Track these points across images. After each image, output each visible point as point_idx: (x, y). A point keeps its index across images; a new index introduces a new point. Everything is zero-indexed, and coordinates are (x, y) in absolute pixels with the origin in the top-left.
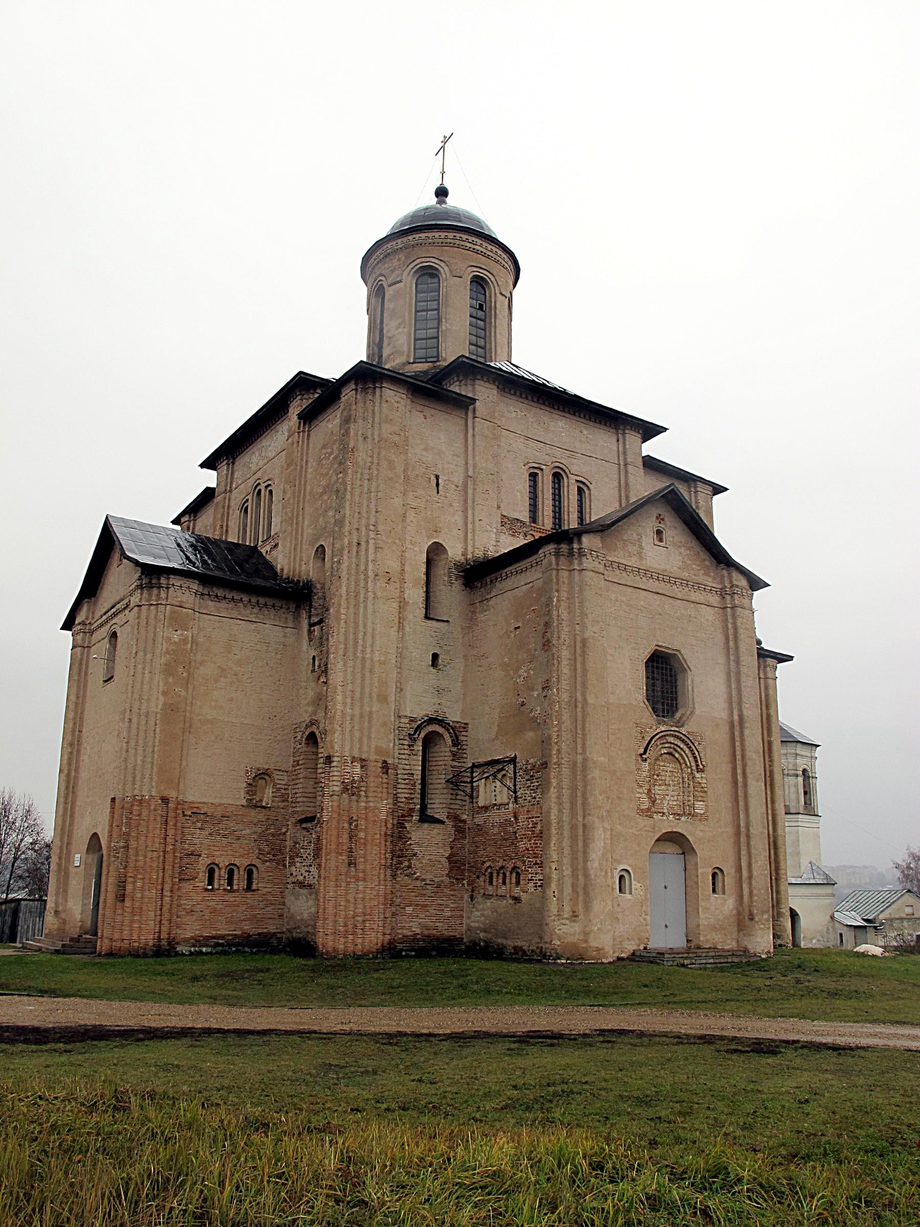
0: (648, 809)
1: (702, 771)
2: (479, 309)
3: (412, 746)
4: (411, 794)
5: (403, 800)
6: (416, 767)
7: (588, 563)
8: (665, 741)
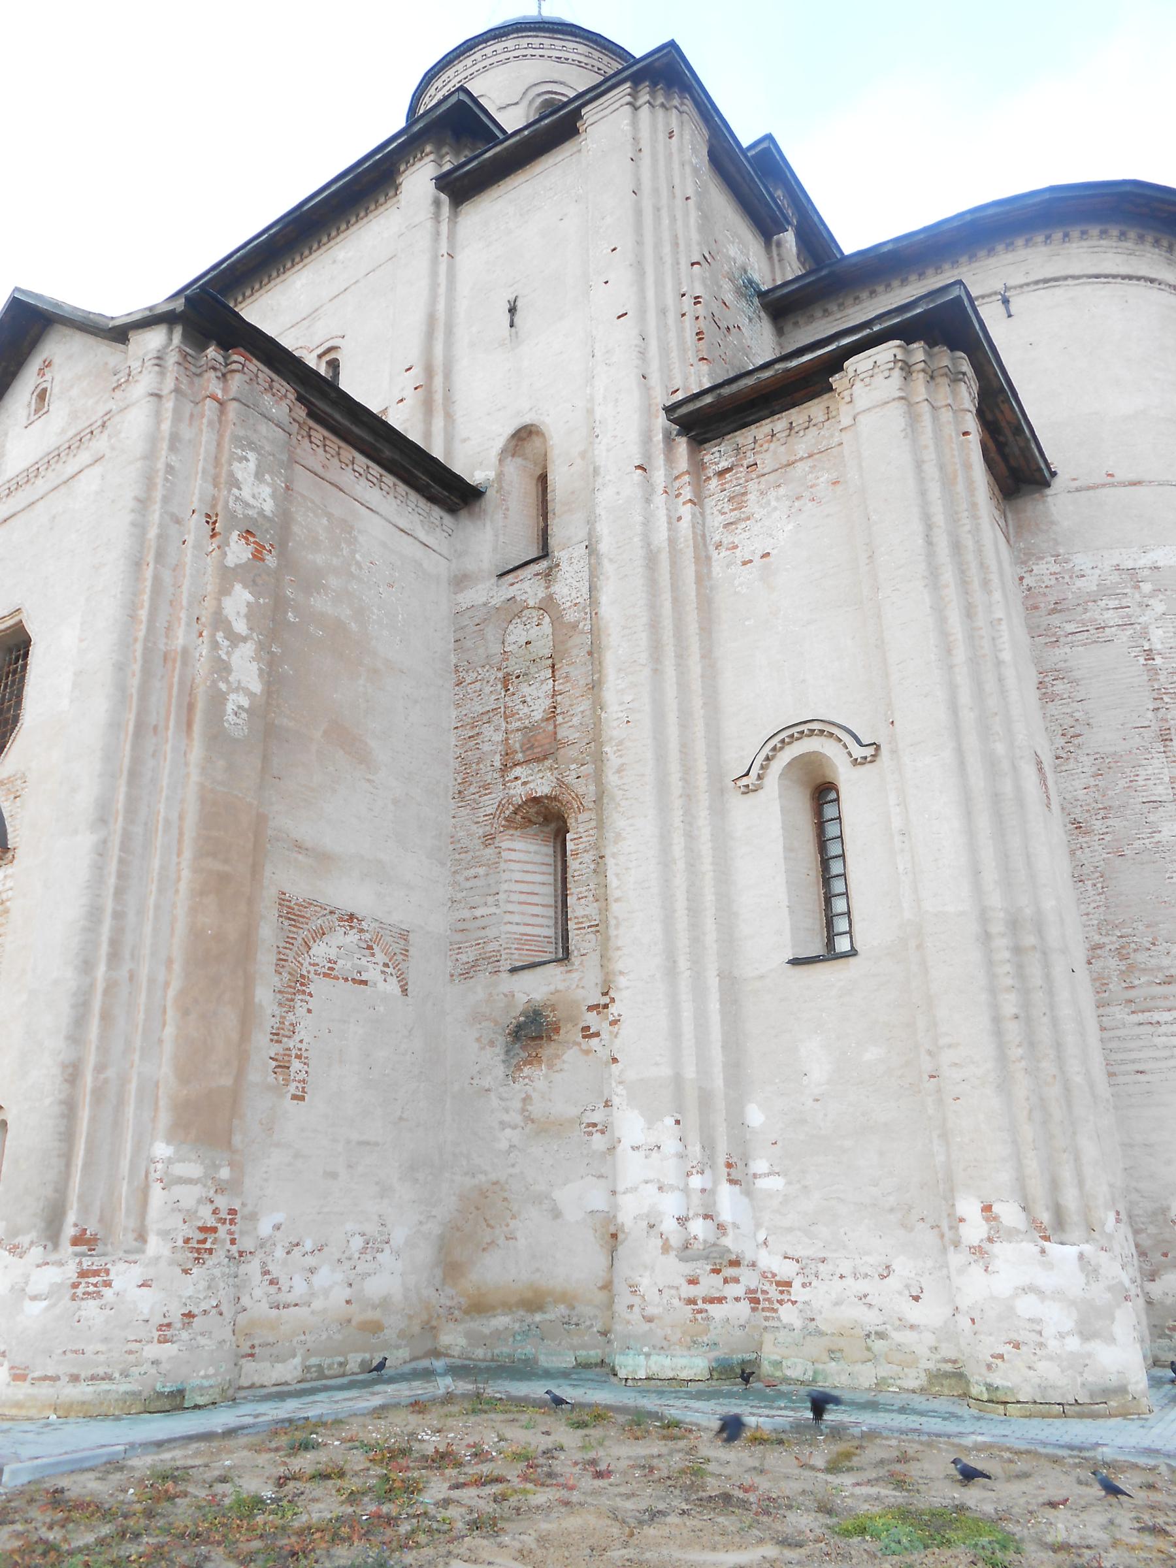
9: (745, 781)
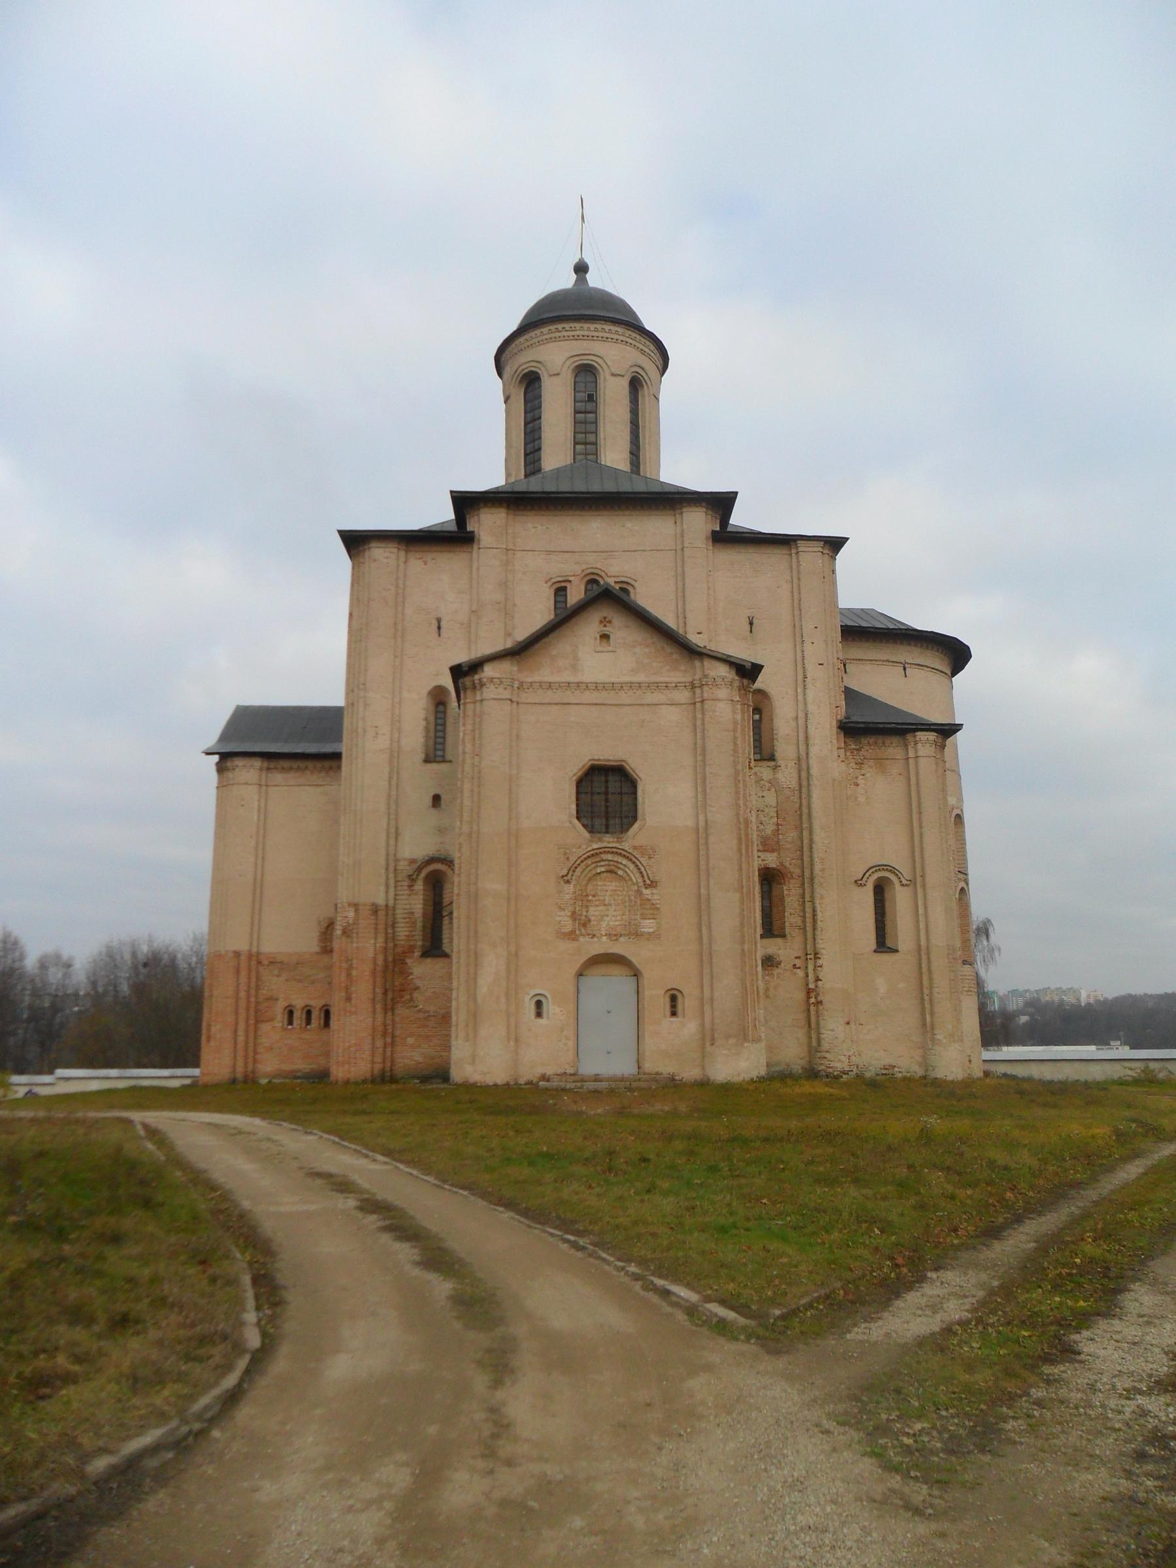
0: (573, 932)
1: (653, 884)
2: (588, 401)
3: (412, 886)
4: (411, 931)
5: (403, 938)
7: (489, 692)
8: (598, 859)
9: (860, 882)
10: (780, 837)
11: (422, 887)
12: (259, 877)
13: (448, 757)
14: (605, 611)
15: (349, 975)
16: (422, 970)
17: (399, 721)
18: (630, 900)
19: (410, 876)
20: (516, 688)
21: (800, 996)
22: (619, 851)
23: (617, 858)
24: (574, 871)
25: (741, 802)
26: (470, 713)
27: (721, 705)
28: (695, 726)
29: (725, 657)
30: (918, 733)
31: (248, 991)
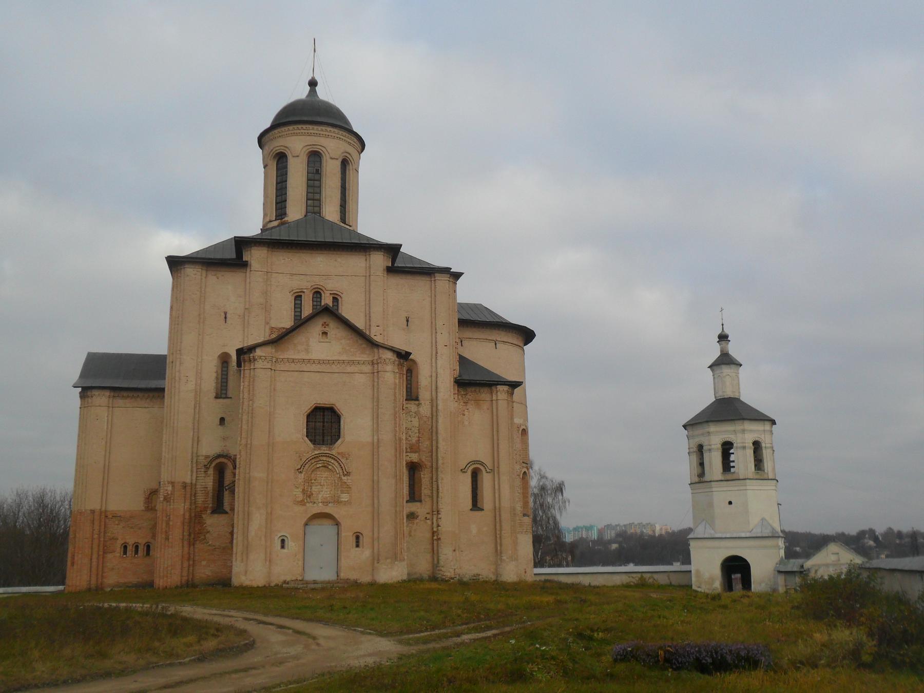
0: (303, 501)
2: (316, 173)
3: (207, 471)
4: (206, 498)
6: (209, 484)
7: (259, 364)
10: (420, 444)
11: (212, 472)
12: (107, 464)
13: (230, 394)
14: (325, 319)
15: (168, 524)
16: (213, 522)
17: (200, 373)
18: (335, 483)
19: (205, 465)
20: (274, 362)
21: (428, 535)
22: (330, 455)
23: (328, 459)
24: (304, 467)
25: (397, 429)
26: (247, 375)
27: (388, 374)
28: (373, 385)
29: (391, 348)
30: (498, 386)
31: (99, 535)
